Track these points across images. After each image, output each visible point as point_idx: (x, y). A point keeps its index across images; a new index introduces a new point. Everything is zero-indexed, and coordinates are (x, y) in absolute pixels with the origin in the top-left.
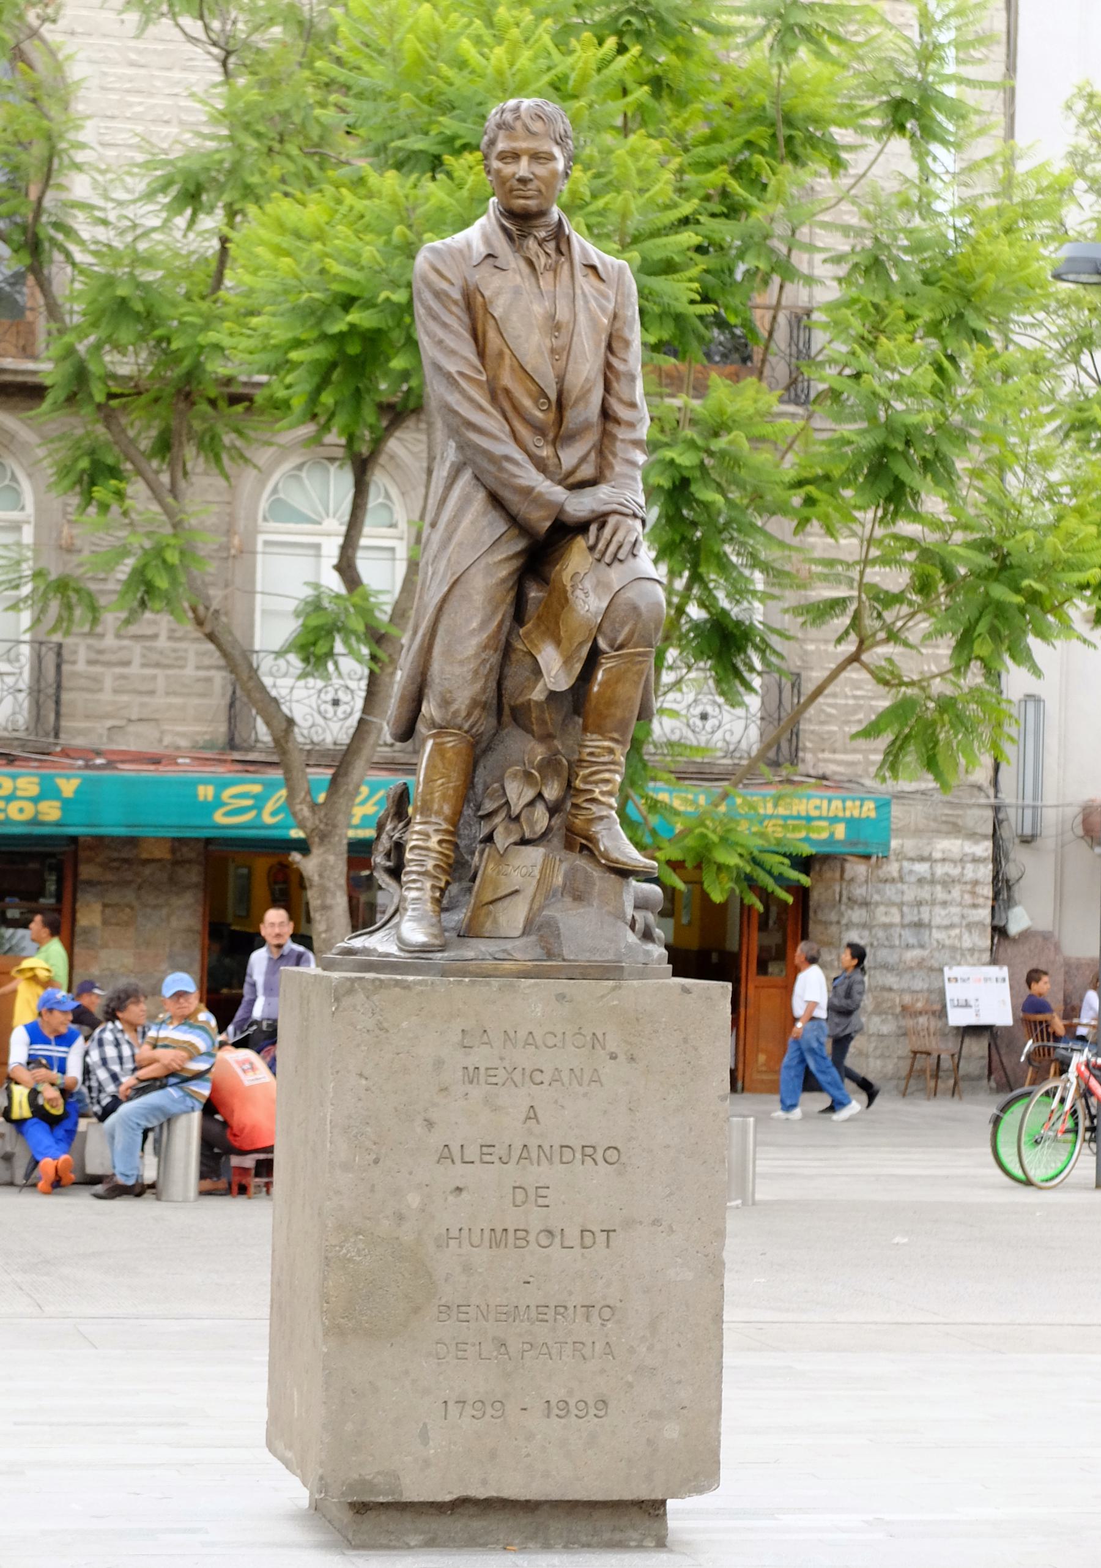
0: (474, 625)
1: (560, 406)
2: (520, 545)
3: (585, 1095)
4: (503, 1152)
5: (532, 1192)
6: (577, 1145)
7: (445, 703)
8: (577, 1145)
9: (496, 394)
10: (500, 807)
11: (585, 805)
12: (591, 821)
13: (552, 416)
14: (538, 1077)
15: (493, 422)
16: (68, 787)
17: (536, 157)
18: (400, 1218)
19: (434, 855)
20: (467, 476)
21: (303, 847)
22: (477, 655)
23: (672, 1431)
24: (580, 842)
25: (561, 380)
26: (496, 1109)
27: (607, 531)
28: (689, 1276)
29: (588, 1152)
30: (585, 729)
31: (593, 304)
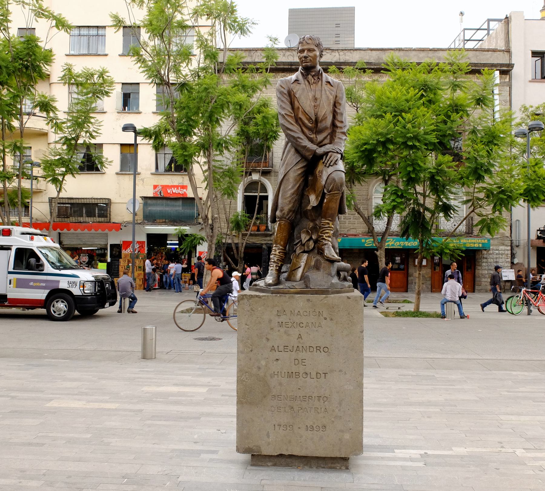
0: (290, 187)
1: (317, 121)
3: (317, 331)
4: (291, 348)
5: (300, 361)
6: (314, 346)
7: (281, 211)
8: (314, 346)
9: (297, 120)
12: (323, 245)
14: (301, 325)
15: (296, 128)
16: (339, 240)
17: (309, 50)
18: (259, 368)
20: (290, 144)
21: (377, 250)
22: (290, 196)
23: (347, 436)
24: (321, 252)
25: (316, 115)
26: (288, 335)
28: (352, 388)
29: (318, 348)
30: (322, 218)
31: (328, 92)
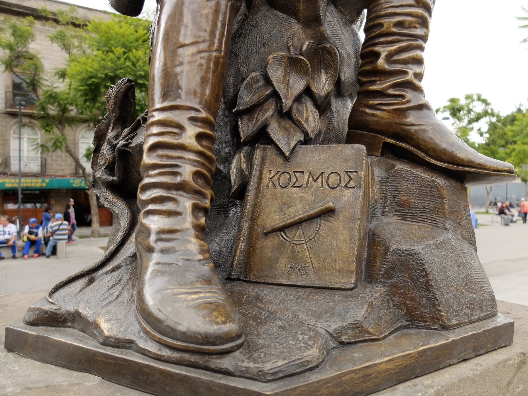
10: (266, 99)
11: (391, 92)
12: (402, 112)
16: (47, 180)
19: (192, 156)
21: (88, 189)
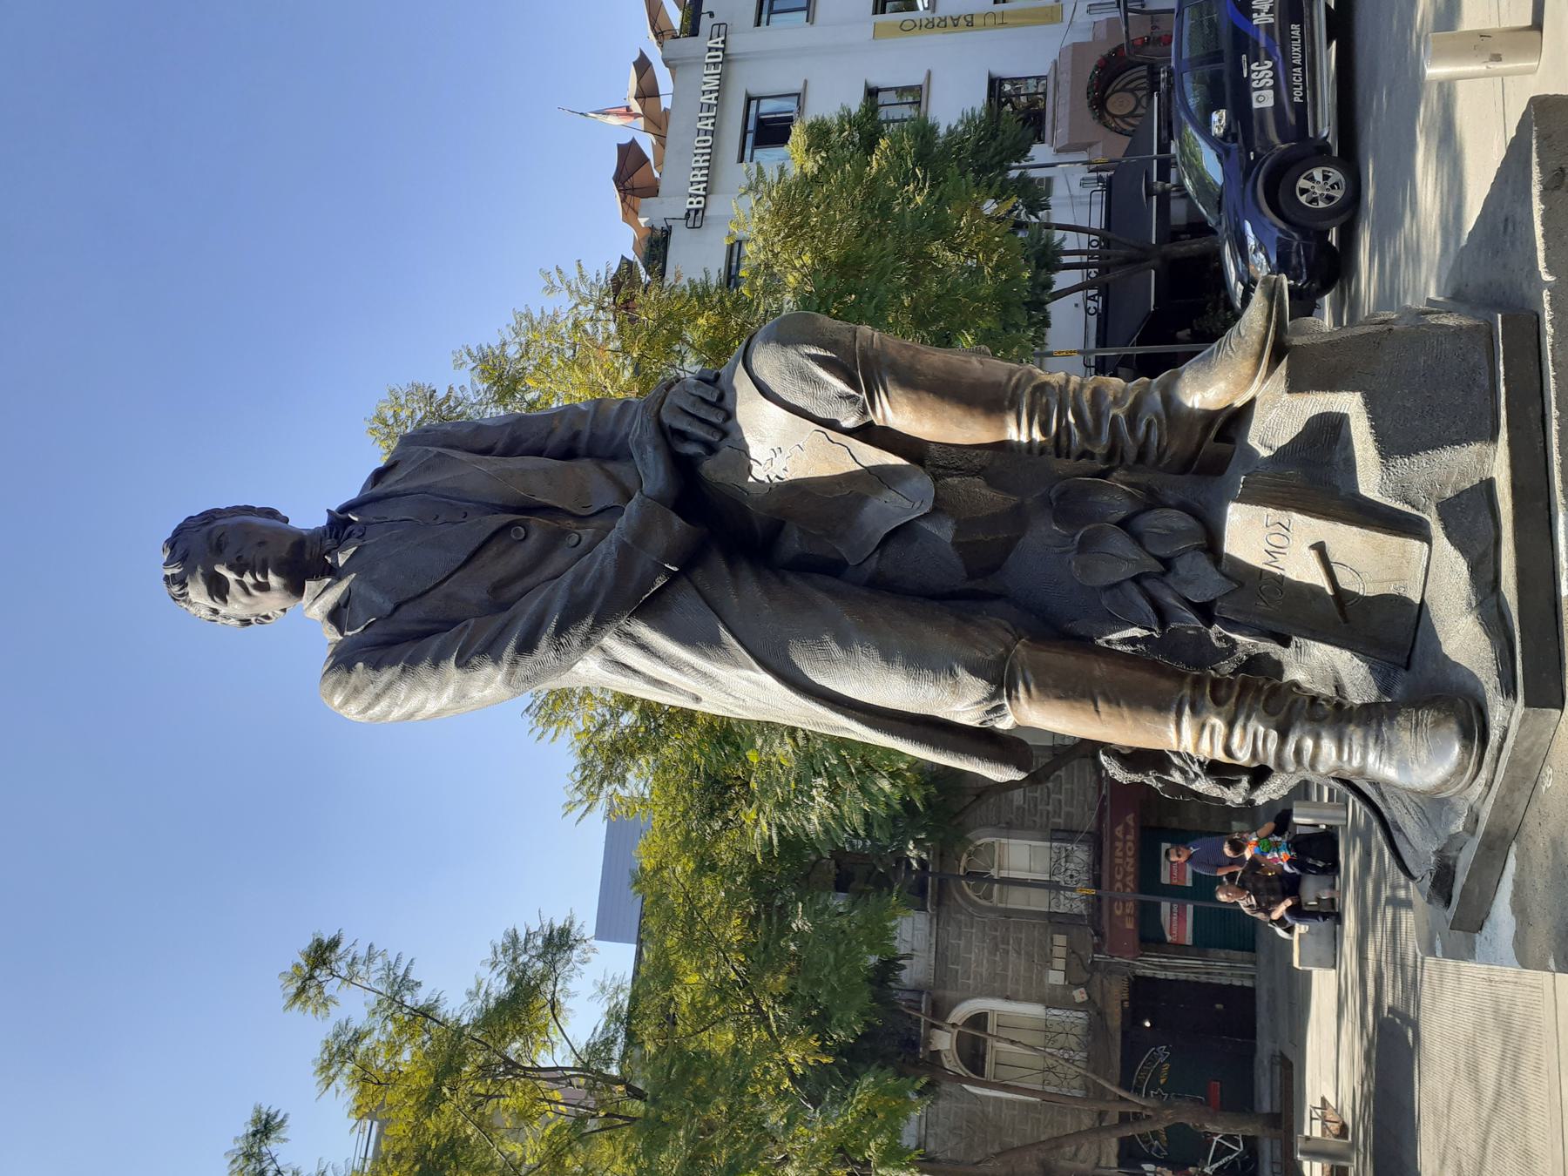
2: (718, 563)
13: (535, 522)
27: (682, 424)
